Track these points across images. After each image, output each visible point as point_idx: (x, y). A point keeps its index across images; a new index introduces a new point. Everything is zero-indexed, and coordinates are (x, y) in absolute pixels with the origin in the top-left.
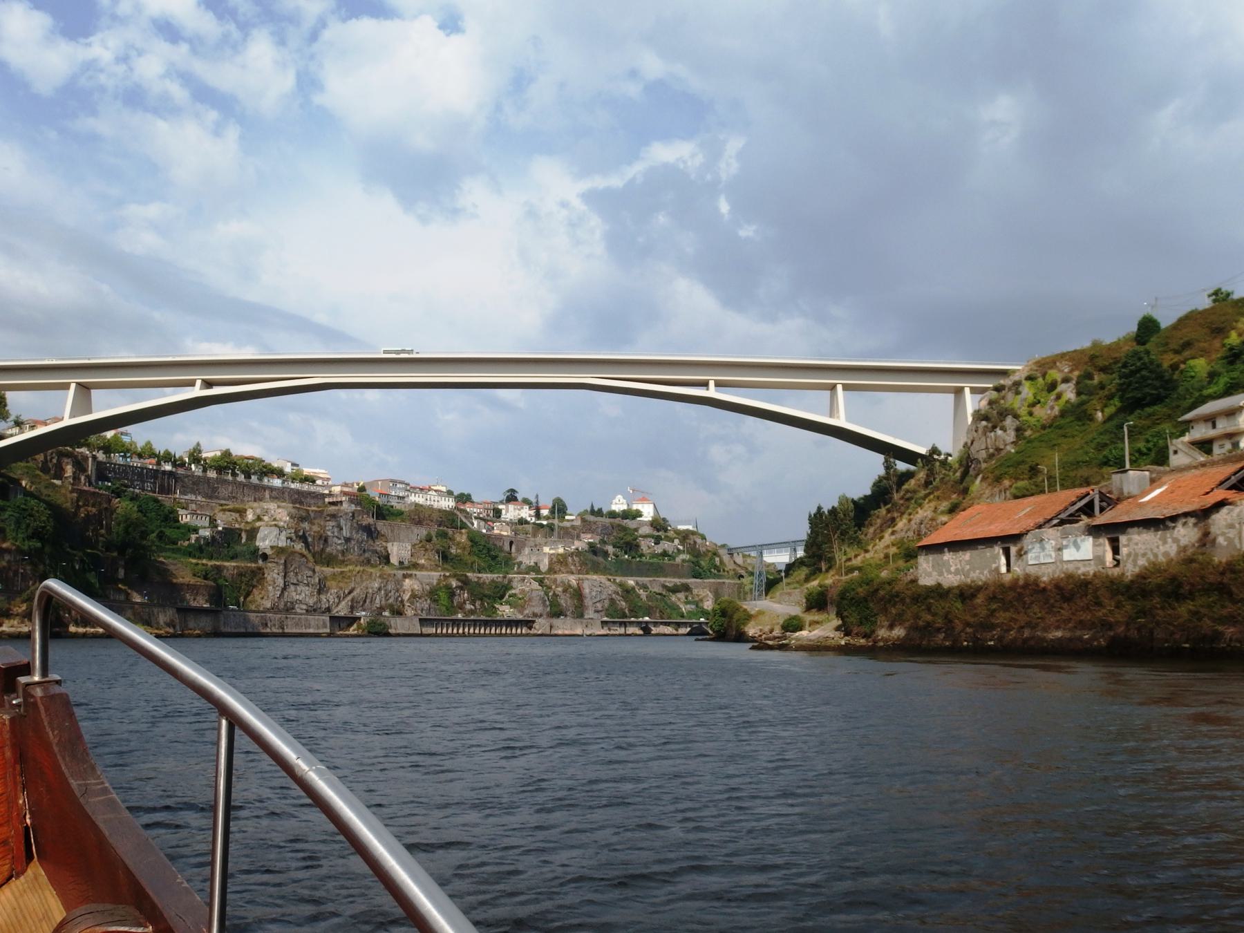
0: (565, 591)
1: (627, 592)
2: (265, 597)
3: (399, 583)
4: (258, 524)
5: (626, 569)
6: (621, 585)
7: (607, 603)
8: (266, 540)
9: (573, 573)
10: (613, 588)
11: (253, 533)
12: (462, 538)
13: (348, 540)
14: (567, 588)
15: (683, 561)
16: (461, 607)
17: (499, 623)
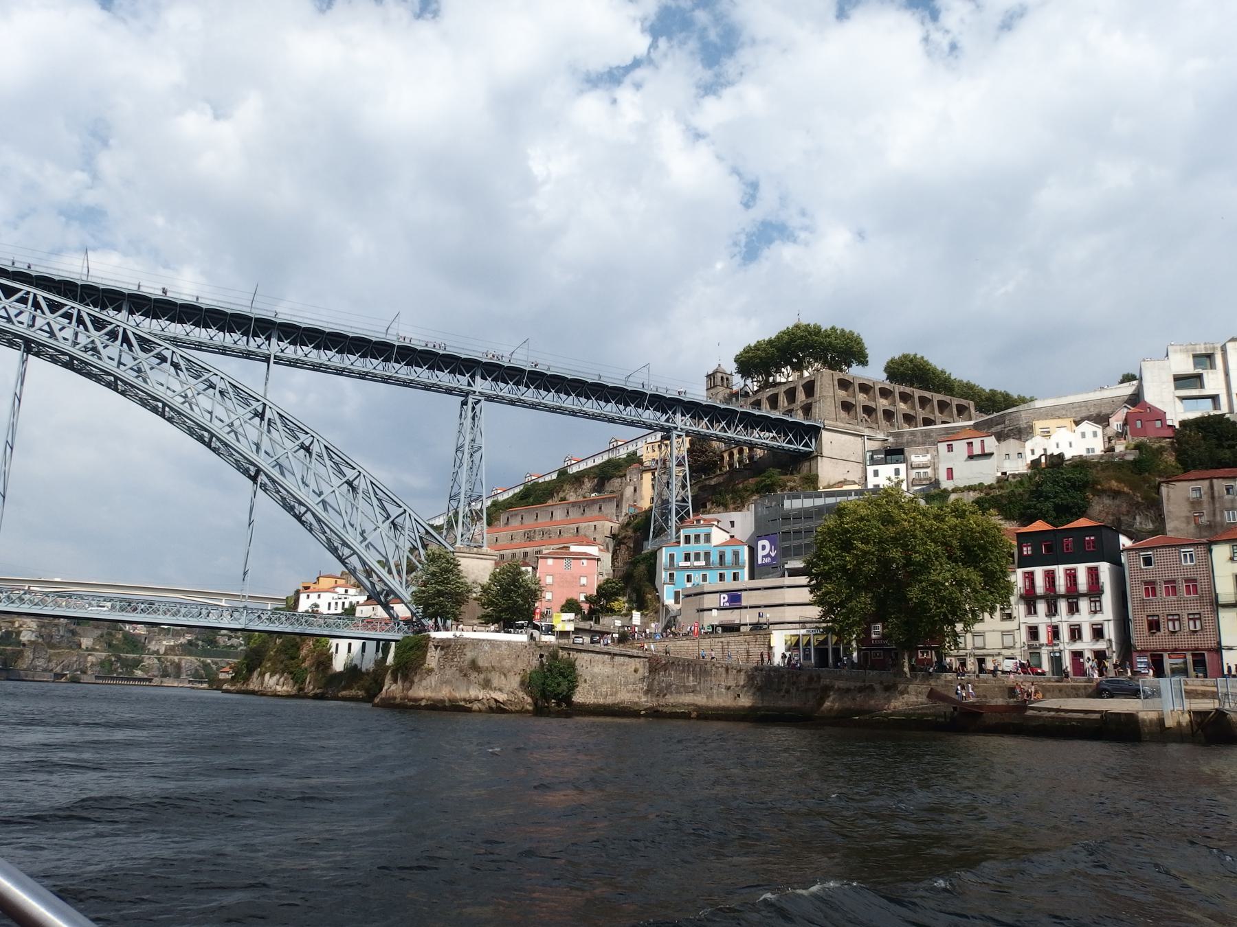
0: (171, 665)
1: (206, 666)
2: (23, 664)
3: (86, 658)
4: (21, 629)
5: (207, 654)
6: (203, 662)
7: (193, 672)
8: (25, 637)
9: (177, 655)
10: (198, 663)
11: (18, 633)
12: (120, 636)
13: (62, 637)
14: (172, 663)
15: (242, 650)
16: (116, 670)
17: (135, 679)
